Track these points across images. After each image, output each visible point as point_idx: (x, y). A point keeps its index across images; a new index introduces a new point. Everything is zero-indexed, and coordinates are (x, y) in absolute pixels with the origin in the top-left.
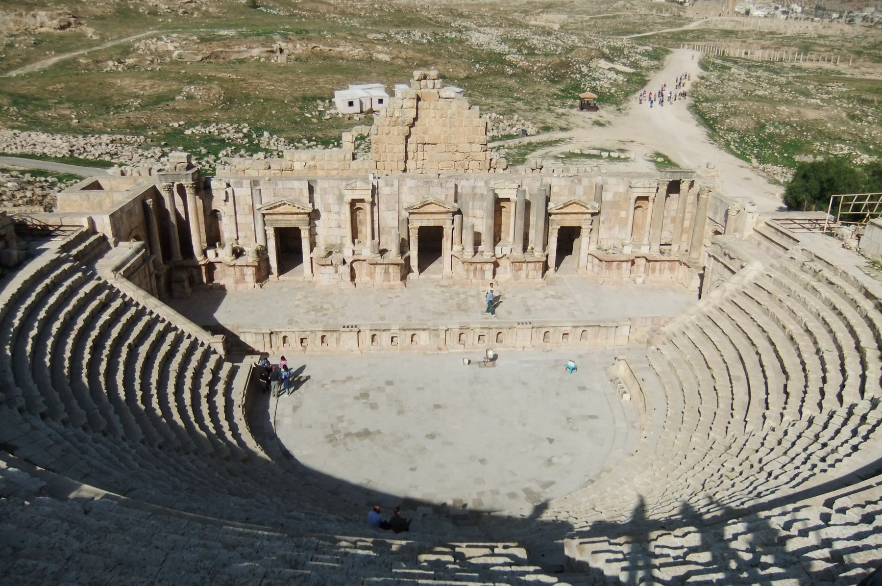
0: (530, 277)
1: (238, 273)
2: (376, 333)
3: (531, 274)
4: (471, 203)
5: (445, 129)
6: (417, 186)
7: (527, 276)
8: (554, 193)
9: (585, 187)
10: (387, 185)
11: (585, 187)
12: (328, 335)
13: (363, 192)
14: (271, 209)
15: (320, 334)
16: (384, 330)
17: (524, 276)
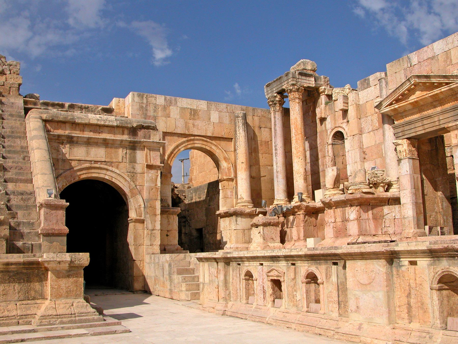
1: (339, 220)
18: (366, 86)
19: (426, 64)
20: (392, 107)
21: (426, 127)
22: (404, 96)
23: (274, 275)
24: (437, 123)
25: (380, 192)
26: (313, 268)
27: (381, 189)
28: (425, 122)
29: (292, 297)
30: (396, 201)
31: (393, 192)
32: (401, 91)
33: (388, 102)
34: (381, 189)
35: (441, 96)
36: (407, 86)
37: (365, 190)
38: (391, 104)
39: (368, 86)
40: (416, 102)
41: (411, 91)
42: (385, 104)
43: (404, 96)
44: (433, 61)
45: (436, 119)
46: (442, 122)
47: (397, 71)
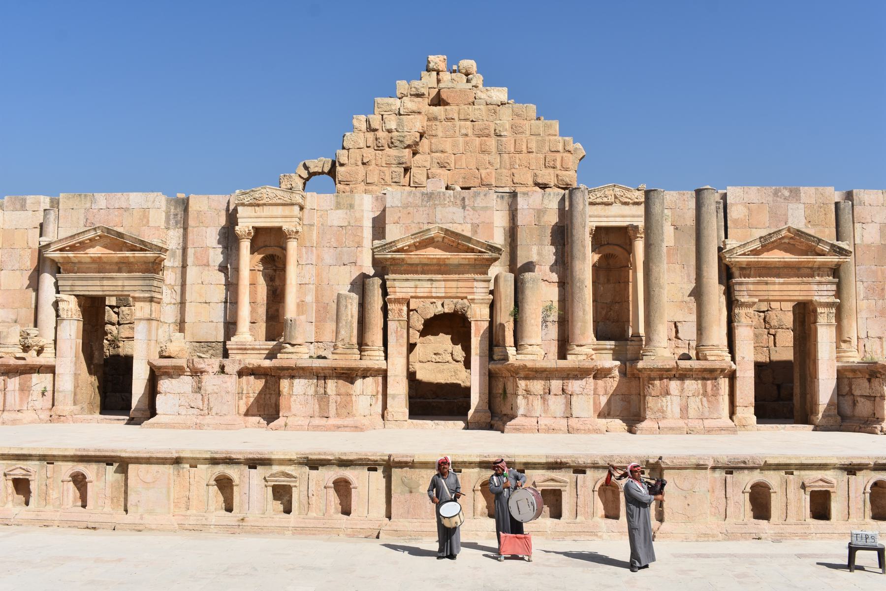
0: (692, 413)
2: (232, 472)
3: (694, 404)
4: (535, 249)
5: (487, 157)
6: (406, 206)
7: (684, 411)
8: (735, 221)
9: (808, 206)
10: (338, 206)
11: (808, 206)
12: (90, 471)
13: (279, 211)
14: (73, 248)
15: (67, 469)
16: (253, 464)
17: (677, 411)
18: (18, 206)
19: (116, 213)
20: (65, 254)
21: (105, 288)
22: (83, 246)
23: (19, 474)
24: (120, 288)
25: (32, 358)
26: (81, 468)
27: (33, 353)
28: (105, 283)
29: (45, 497)
30: (51, 369)
31: (47, 358)
32: (82, 238)
33: (60, 246)
34: (33, 353)
35: (132, 260)
36: (91, 235)
37: (18, 355)
38: (61, 250)
39: (23, 207)
40: (100, 258)
41: (92, 242)
42: (53, 247)
43: (83, 246)
44: (126, 214)
45: (120, 283)
46: (126, 288)
47: (75, 207)
